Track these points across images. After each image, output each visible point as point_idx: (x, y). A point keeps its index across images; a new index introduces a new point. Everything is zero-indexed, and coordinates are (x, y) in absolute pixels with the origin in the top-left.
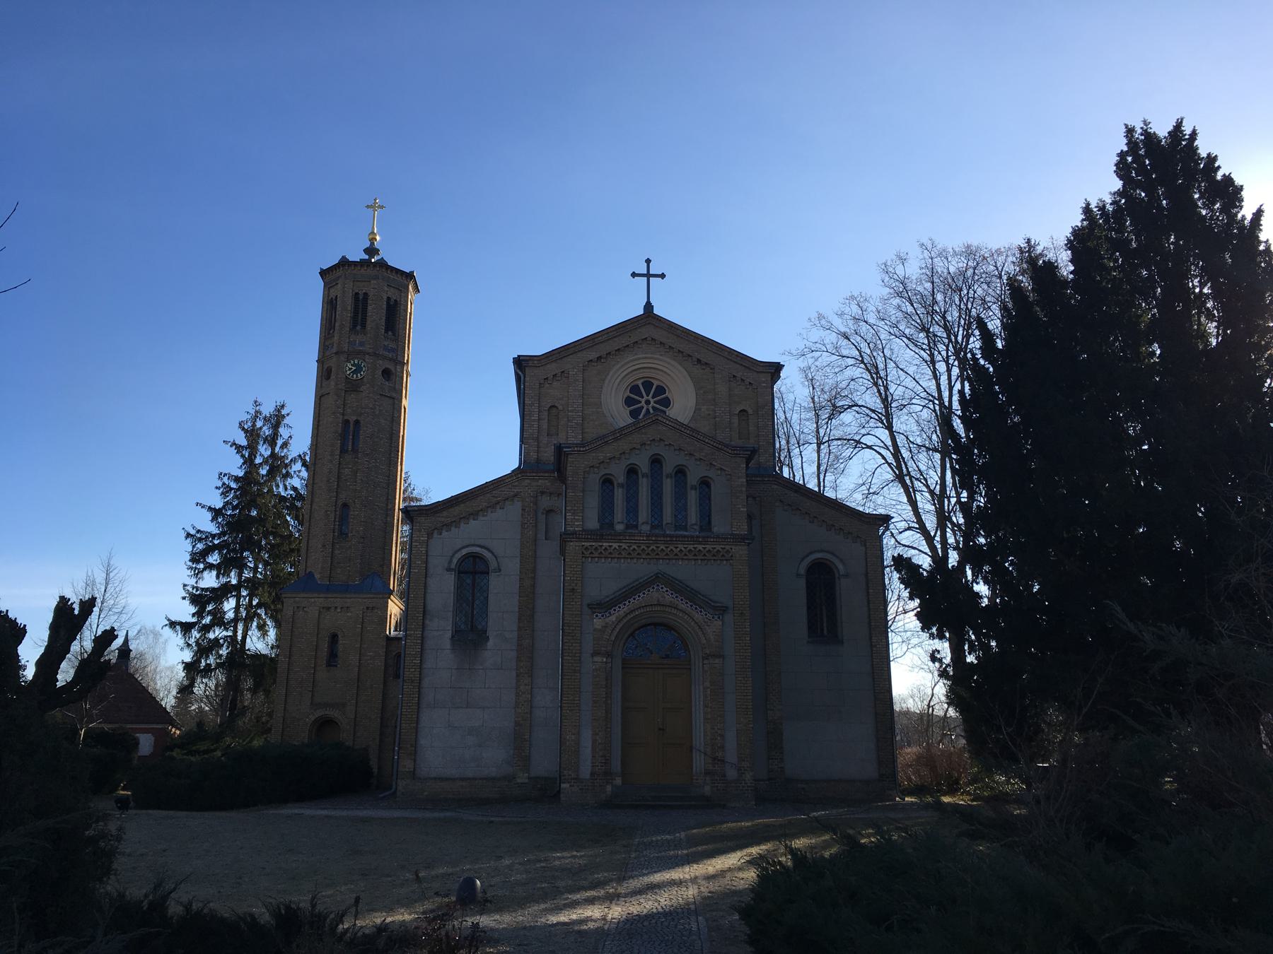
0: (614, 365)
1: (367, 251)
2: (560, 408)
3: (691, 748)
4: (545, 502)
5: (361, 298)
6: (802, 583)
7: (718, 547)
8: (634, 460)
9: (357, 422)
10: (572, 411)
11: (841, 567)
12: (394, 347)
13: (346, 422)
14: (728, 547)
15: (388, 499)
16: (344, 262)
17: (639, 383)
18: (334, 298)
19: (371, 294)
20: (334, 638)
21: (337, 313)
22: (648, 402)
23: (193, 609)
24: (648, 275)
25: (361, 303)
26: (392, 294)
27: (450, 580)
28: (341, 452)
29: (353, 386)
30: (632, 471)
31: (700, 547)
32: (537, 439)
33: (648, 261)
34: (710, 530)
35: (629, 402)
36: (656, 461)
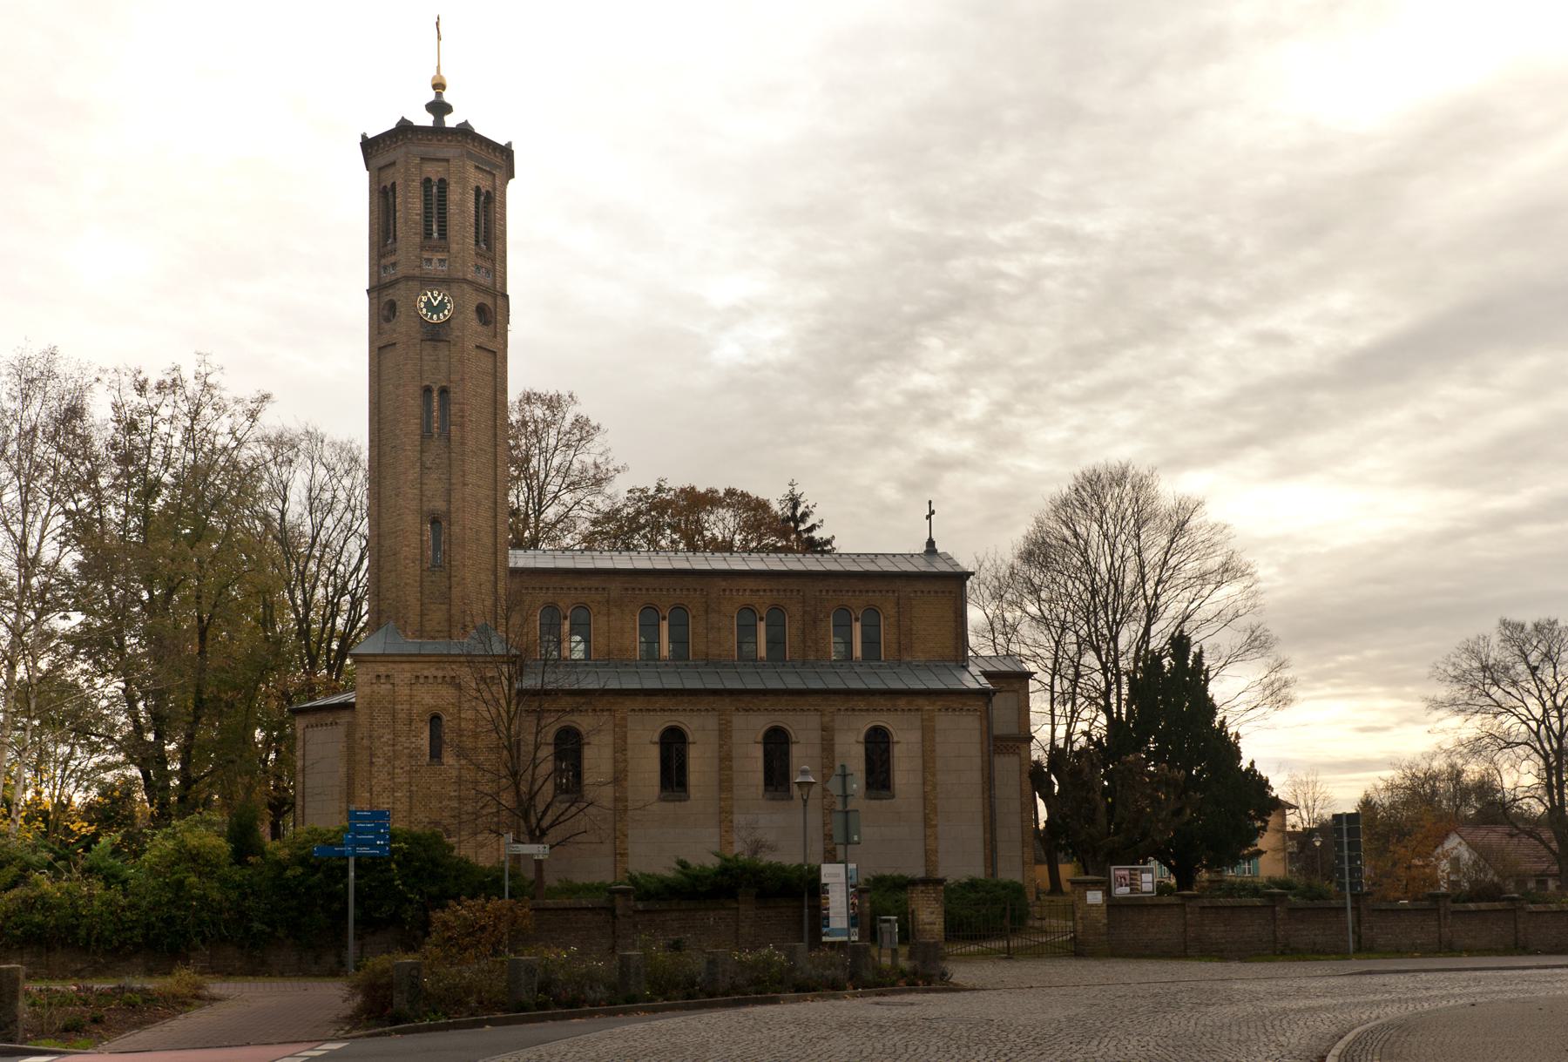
16: (405, 129)
18: (389, 186)
26: (485, 185)
29: (435, 335)
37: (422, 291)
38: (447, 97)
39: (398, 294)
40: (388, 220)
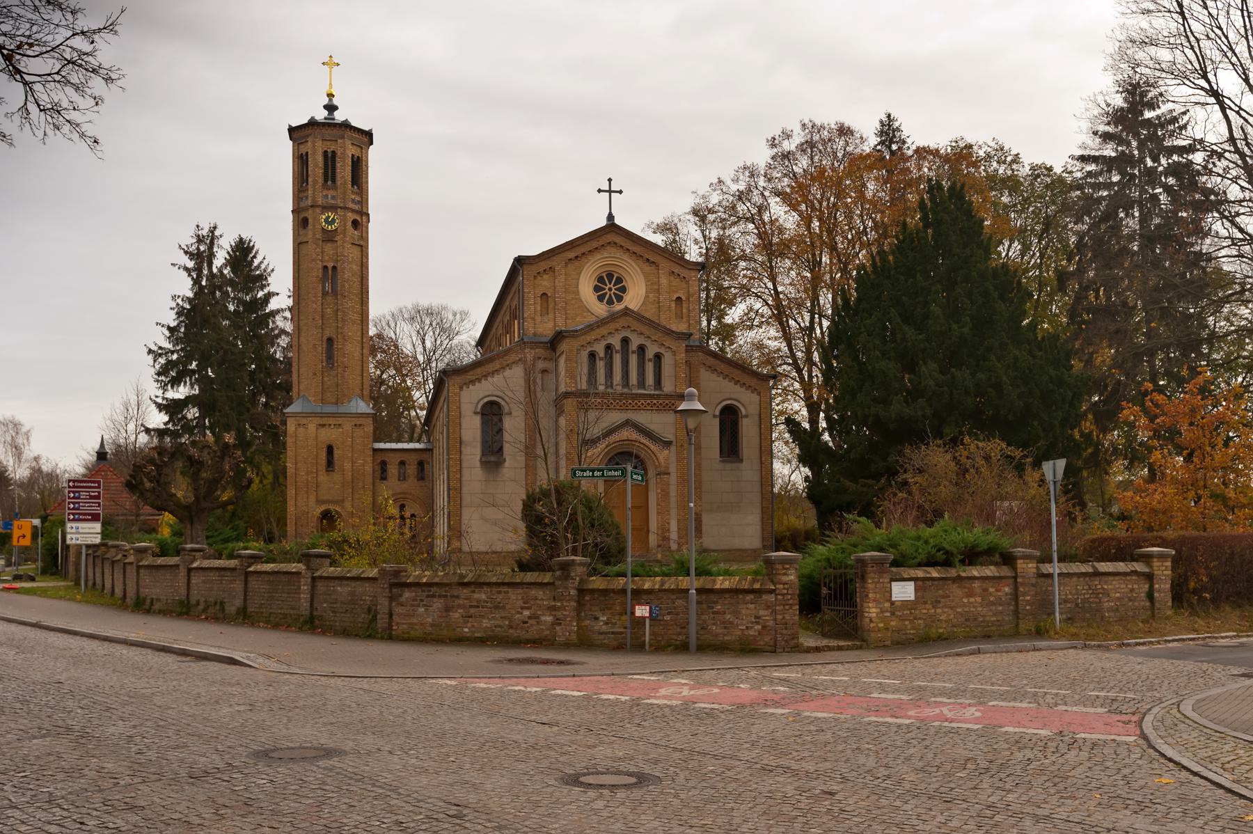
0: (587, 263)
1: (326, 107)
2: (549, 295)
3: (648, 531)
4: (541, 365)
5: (330, 155)
6: (717, 420)
7: (667, 402)
8: (610, 340)
9: (334, 268)
10: (558, 298)
11: (743, 410)
12: (360, 199)
13: (325, 268)
14: (673, 401)
15: (362, 334)
16: (312, 123)
17: (604, 275)
19: (339, 153)
20: (330, 450)
21: (309, 169)
22: (610, 289)
23: (166, 418)
24: (610, 191)
25: (330, 160)
26: (357, 152)
27: (477, 421)
28: (323, 294)
29: (329, 237)
30: (609, 347)
31: (655, 401)
32: (534, 319)
33: (610, 180)
34: (660, 389)
35: (597, 289)
36: (625, 341)
37: (323, 213)
38: (335, 101)
39: (309, 214)
40: (303, 168)
